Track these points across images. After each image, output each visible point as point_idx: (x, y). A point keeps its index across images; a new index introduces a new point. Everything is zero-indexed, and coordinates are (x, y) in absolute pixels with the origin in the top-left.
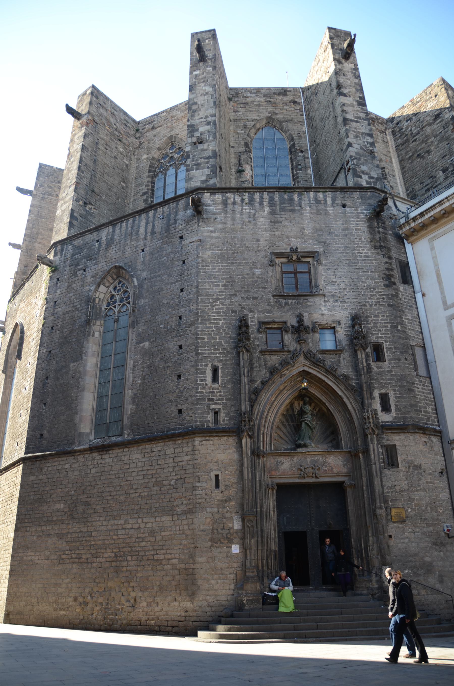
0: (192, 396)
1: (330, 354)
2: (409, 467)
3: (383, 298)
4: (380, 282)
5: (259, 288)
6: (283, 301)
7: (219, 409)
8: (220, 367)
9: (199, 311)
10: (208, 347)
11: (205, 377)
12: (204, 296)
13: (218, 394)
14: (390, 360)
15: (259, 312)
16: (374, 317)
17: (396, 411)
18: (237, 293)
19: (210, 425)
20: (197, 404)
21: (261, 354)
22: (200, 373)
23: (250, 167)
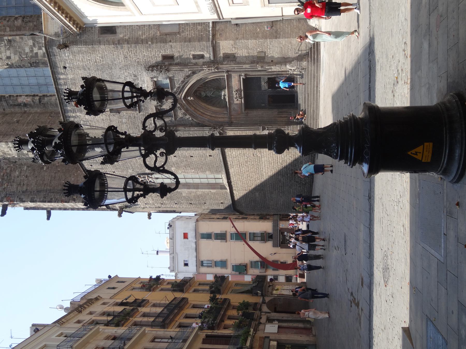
3: (131, 51)
23: (19, 98)
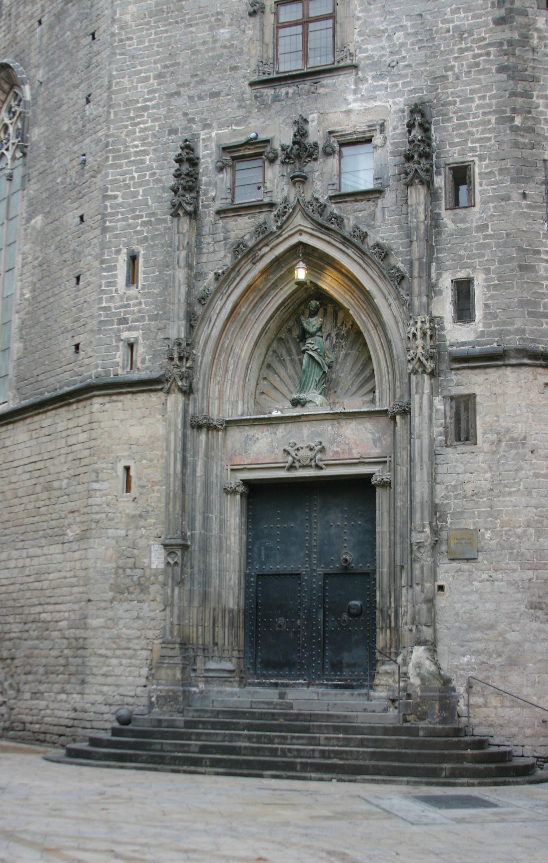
0: (92, 316)
1: (356, 201)
2: (500, 441)
3: (488, 54)
4: (487, 14)
5: (225, 71)
6: (269, 92)
7: (137, 339)
8: (142, 252)
9: (110, 140)
10: (122, 214)
11: (115, 276)
12: (119, 105)
13: (136, 309)
14: (485, 202)
15: (221, 126)
16: (461, 103)
17: (485, 318)
18: (182, 90)
19: (120, 371)
20: (99, 331)
21: (218, 218)
22: (105, 270)
